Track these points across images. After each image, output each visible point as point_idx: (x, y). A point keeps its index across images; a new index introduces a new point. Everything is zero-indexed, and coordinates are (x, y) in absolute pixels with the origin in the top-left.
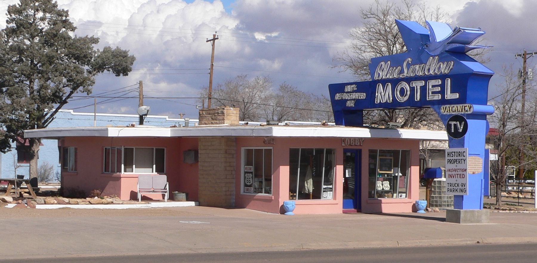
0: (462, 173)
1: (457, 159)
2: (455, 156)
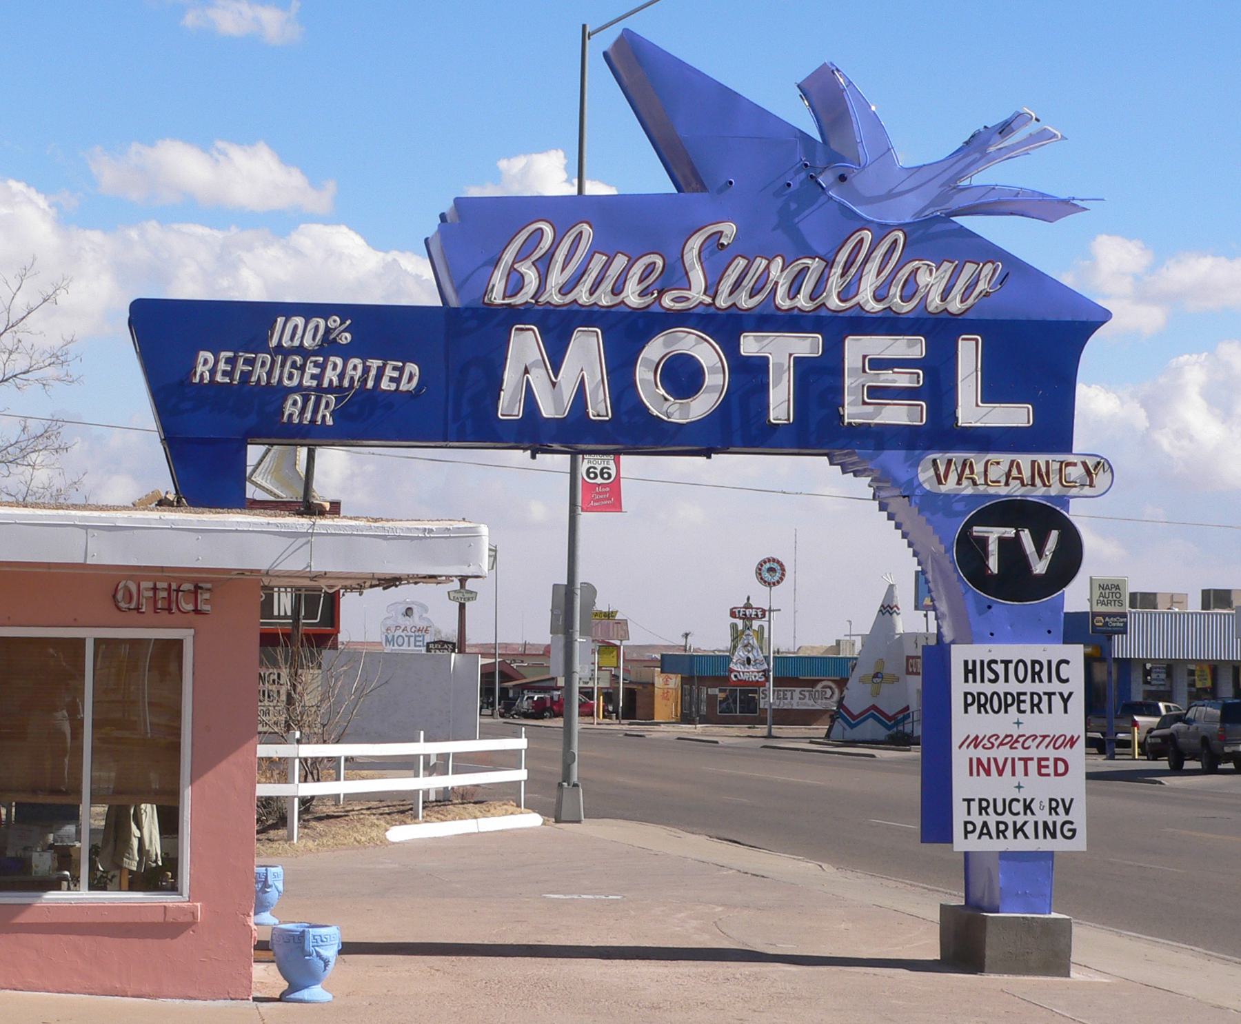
0: (1051, 753)
1: (1019, 694)
2: (1006, 680)
